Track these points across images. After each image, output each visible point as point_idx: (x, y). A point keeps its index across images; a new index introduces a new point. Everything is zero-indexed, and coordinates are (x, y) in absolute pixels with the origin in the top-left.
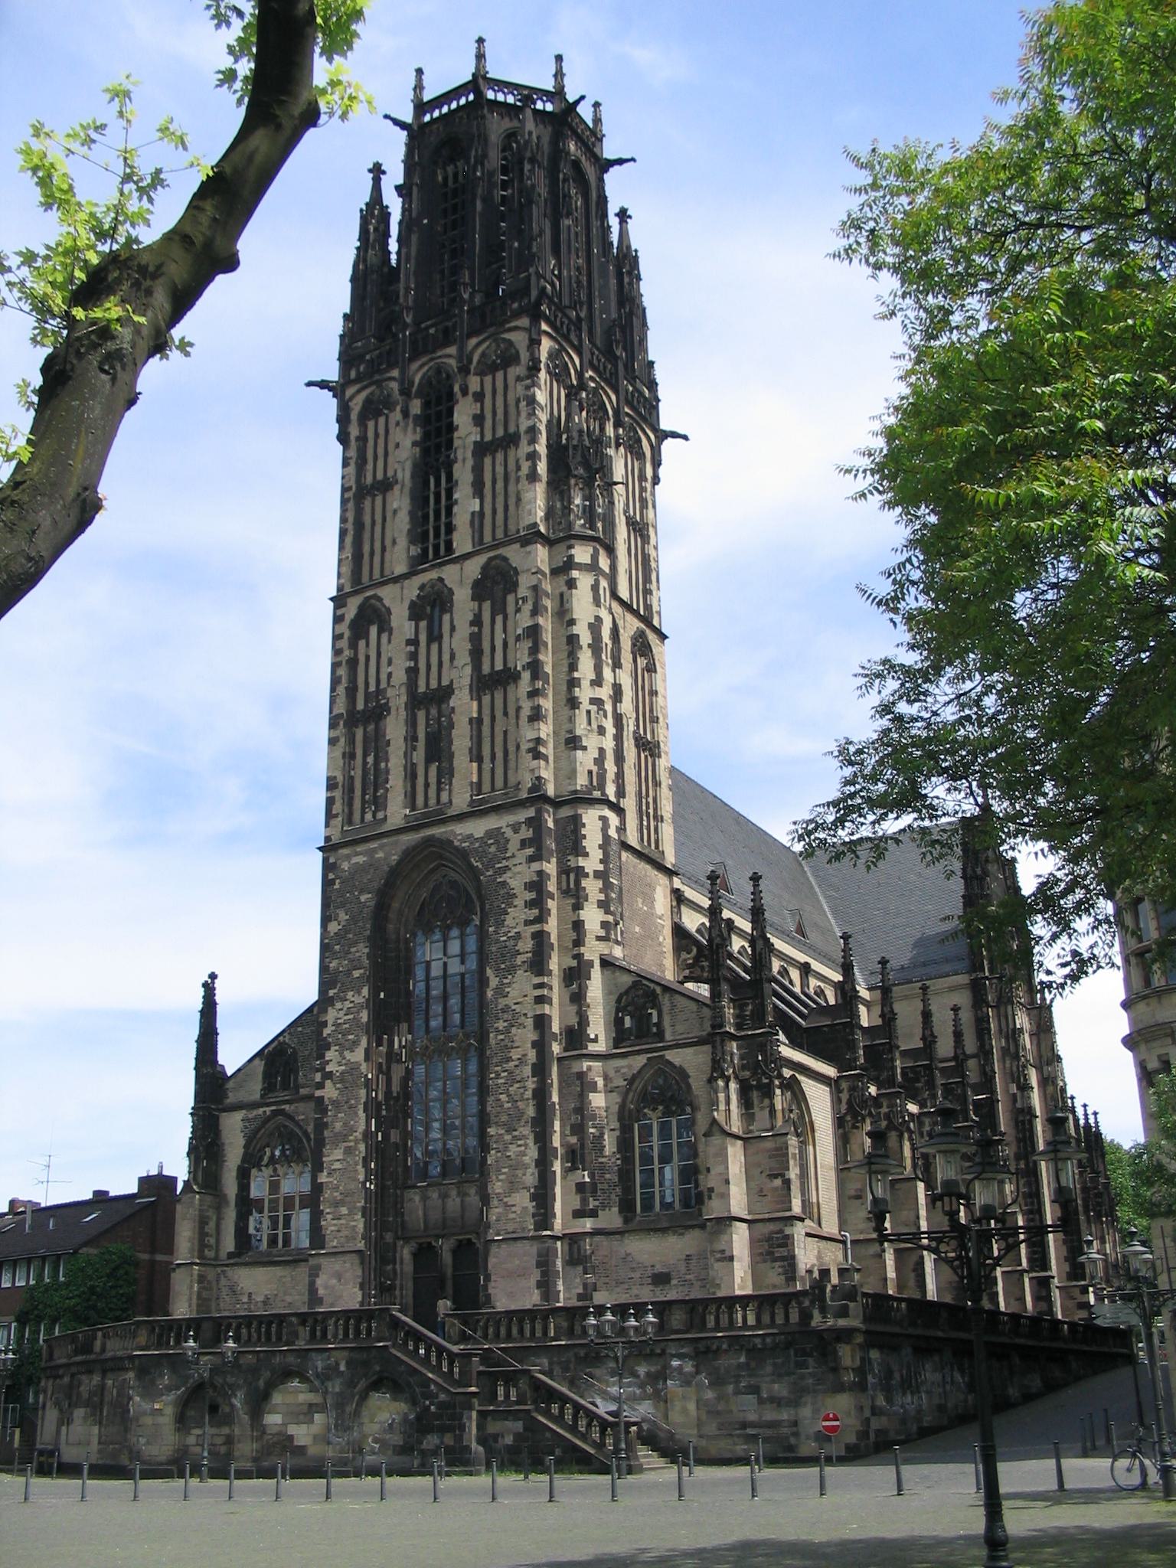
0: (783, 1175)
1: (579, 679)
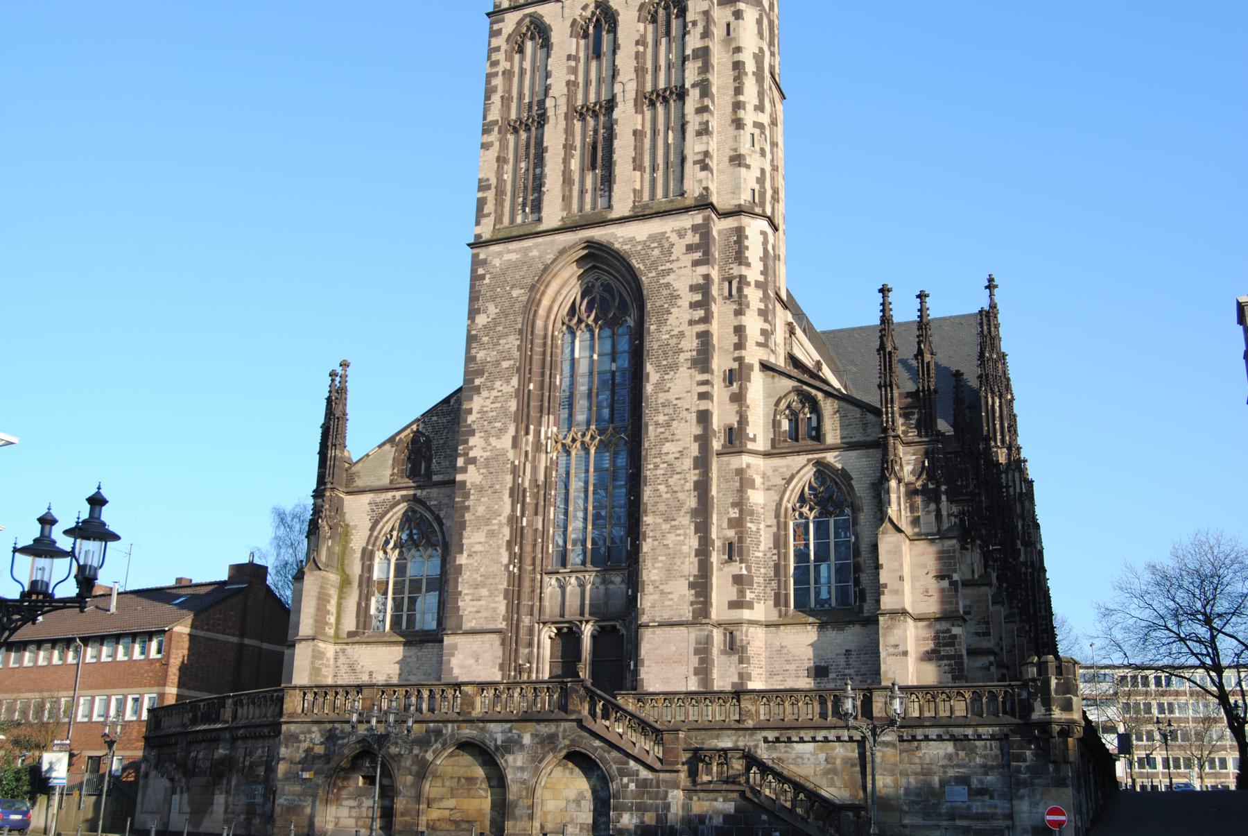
0: (950, 577)
1: (744, 103)
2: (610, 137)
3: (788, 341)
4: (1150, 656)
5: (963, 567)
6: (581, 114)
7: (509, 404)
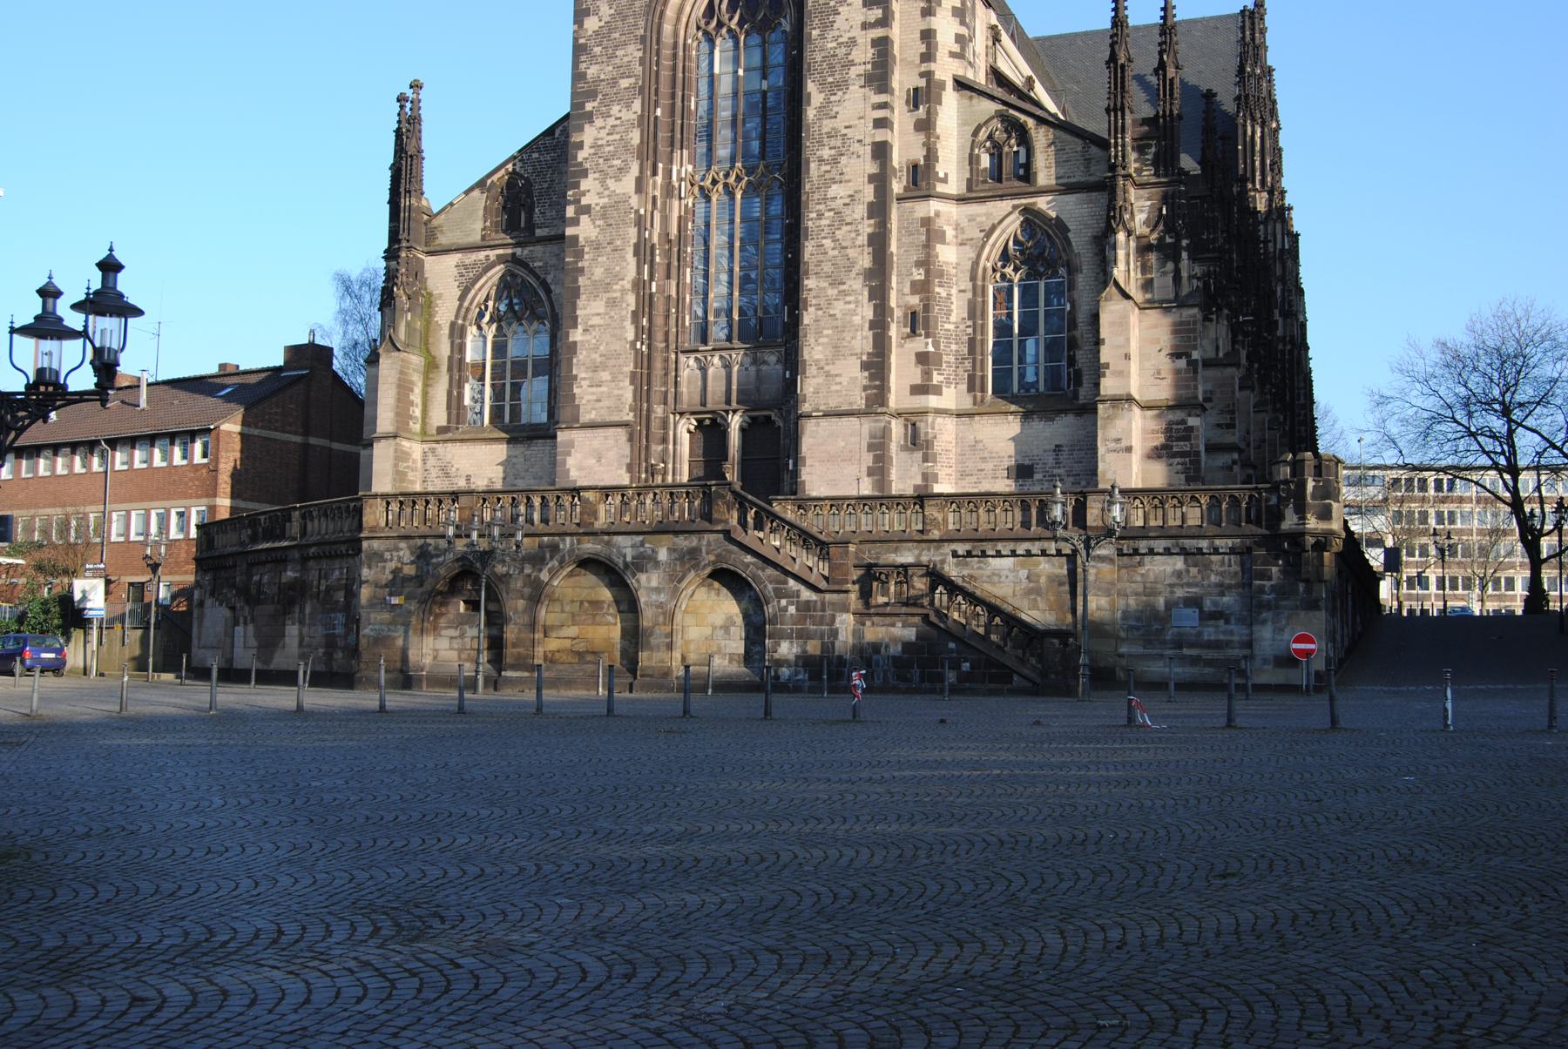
0: (1188, 355)
3: (991, 51)
4: (1431, 454)
5: (1205, 342)
7: (631, 135)
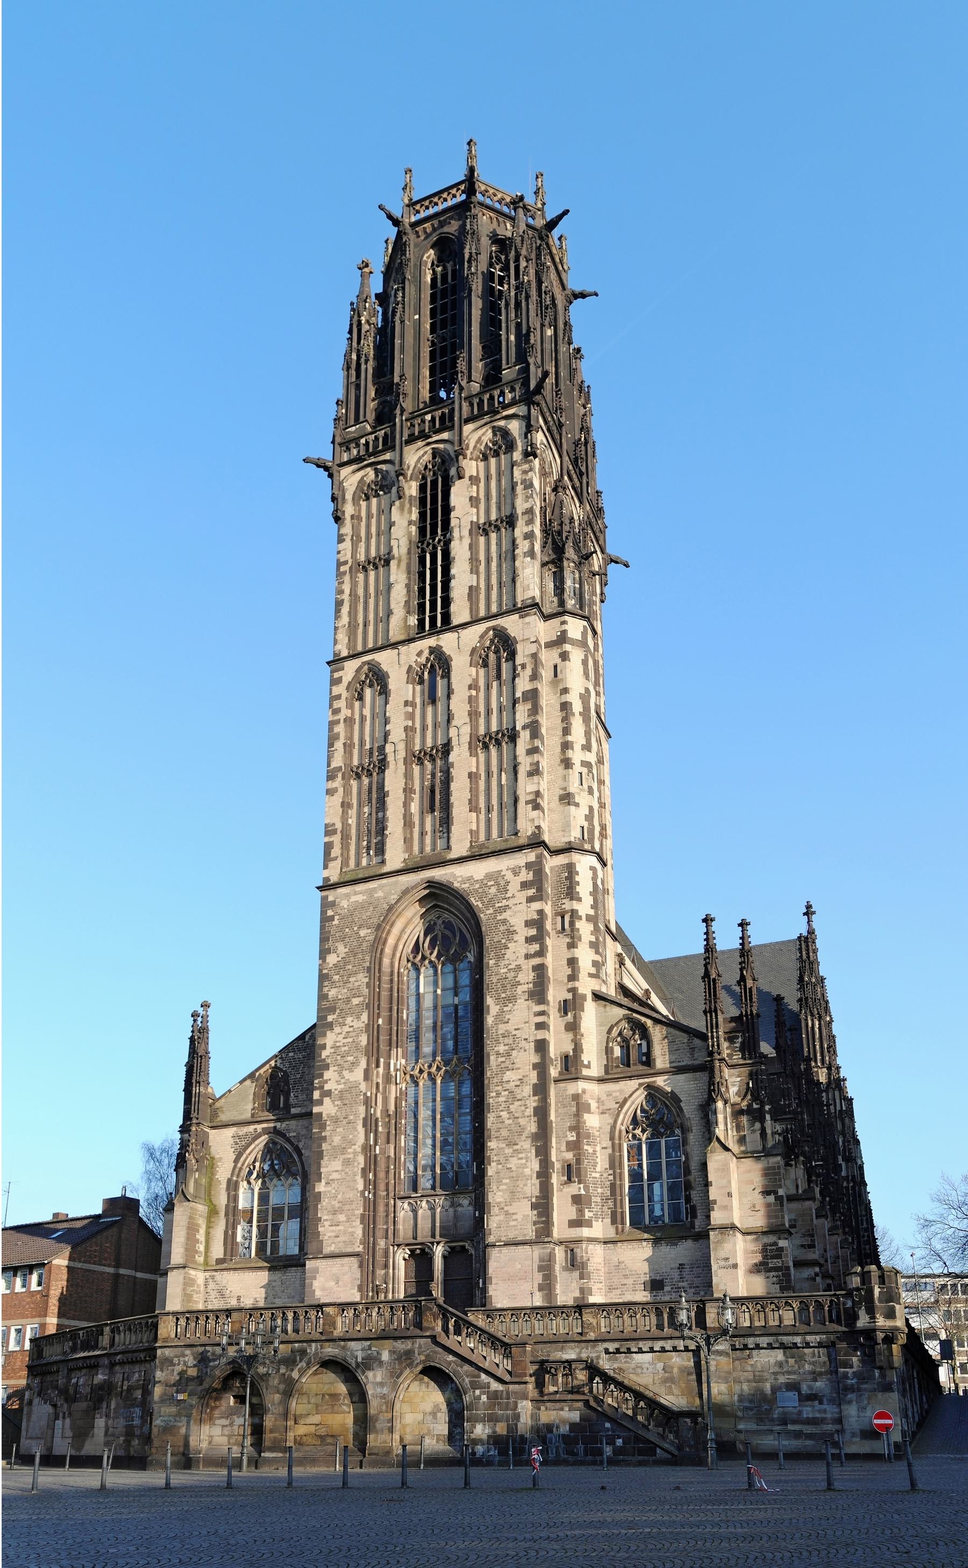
1: (572, 743)
2: (447, 780)
3: (618, 972)
5: (788, 1182)
6: (419, 759)
